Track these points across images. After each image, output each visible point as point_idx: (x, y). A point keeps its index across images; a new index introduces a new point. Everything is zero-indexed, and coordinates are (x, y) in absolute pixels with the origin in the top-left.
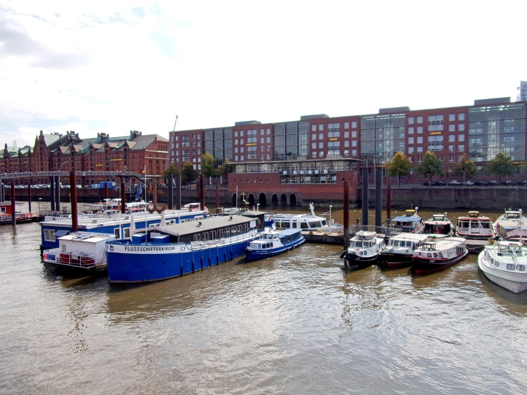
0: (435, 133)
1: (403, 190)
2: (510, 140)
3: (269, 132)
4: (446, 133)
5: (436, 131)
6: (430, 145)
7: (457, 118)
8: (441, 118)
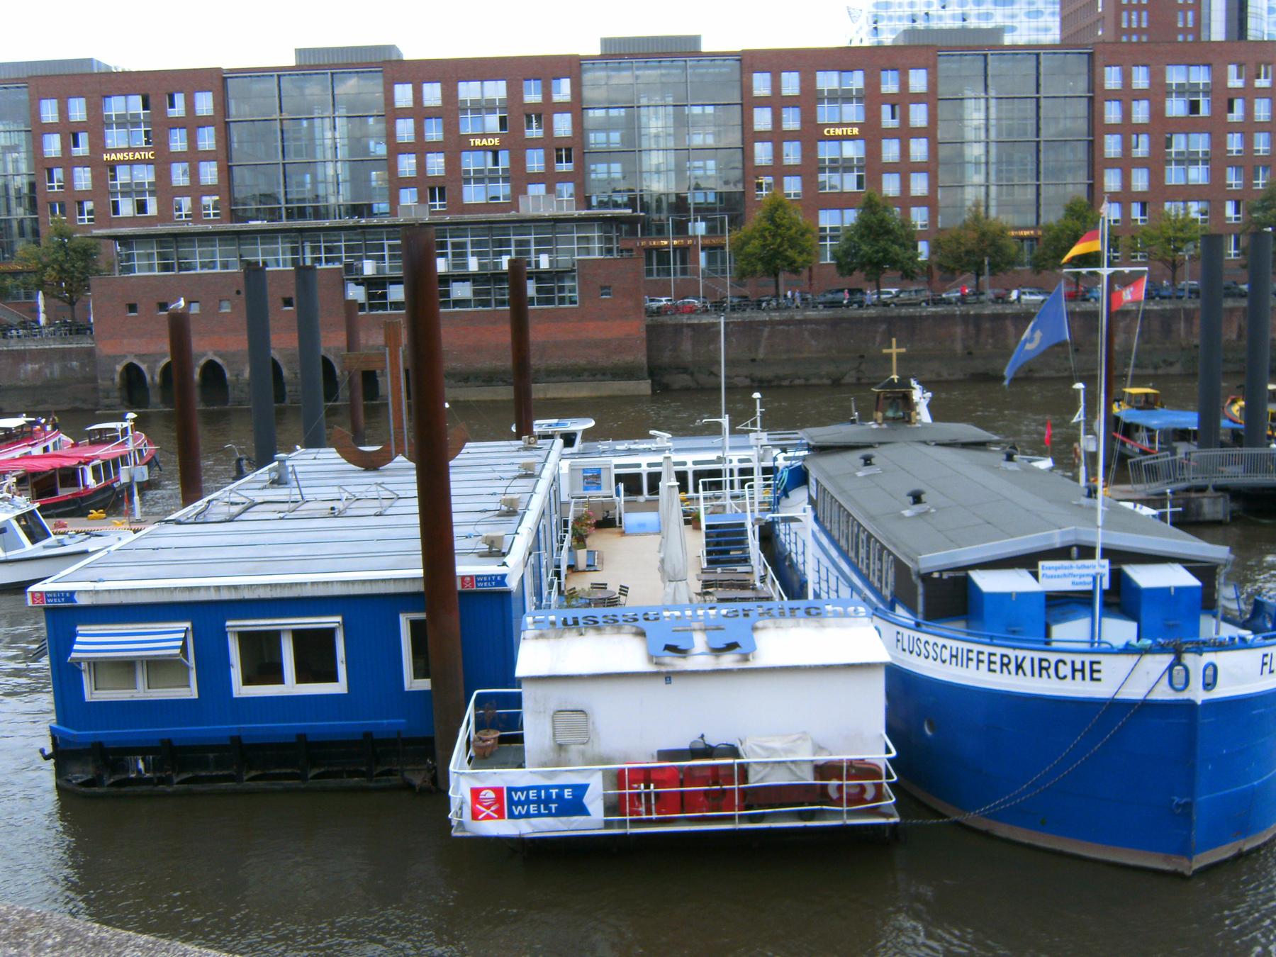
0: (839, 132)
1: (800, 322)
2: (704, 168)
3: (205, 104)
4: (871, 133)
5: (841, 125)
6: (822, 170)
7: (904, 84)
8: (497, 90)
